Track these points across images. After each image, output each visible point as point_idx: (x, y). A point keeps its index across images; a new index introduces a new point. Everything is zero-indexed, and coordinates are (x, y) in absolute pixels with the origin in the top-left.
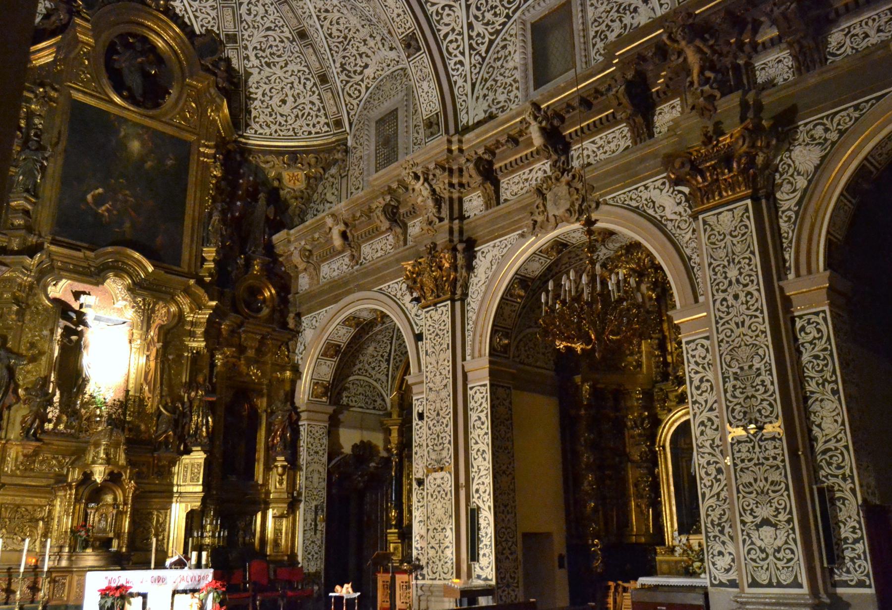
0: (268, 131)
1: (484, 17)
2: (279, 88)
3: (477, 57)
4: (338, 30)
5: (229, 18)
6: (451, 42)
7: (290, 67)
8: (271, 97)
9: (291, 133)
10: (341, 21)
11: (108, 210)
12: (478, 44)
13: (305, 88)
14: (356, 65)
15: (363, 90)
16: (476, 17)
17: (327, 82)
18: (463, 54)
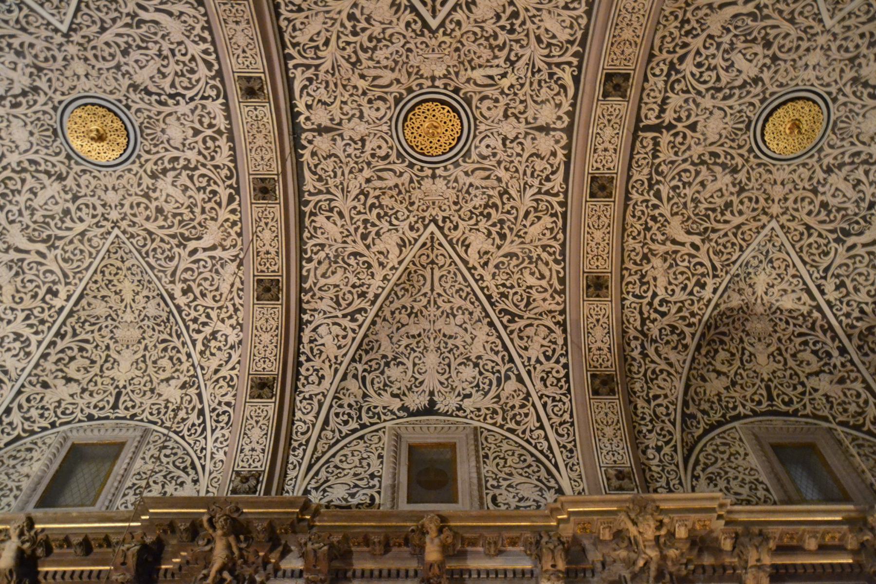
1: (28, 410)
16: (20, 407)
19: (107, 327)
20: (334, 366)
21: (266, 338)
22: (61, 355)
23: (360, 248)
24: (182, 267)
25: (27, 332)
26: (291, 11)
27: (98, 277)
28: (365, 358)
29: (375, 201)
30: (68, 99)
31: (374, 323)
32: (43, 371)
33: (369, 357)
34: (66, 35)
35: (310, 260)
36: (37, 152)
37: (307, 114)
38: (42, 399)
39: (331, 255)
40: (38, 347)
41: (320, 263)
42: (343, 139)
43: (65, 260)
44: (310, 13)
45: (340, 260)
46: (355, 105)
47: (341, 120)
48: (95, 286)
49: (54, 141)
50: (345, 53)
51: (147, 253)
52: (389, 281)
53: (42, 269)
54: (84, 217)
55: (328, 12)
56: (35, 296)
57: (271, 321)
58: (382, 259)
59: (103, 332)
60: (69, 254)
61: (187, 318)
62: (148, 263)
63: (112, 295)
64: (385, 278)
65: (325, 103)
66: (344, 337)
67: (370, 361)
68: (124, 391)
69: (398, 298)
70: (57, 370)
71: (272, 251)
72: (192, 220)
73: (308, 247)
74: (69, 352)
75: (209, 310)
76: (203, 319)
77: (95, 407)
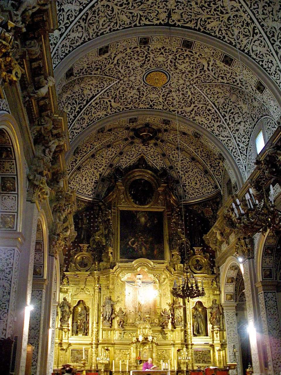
0: (194, 196)
3: (244, 156)
5: (168, 161)
6: (234, 152)
7: (194, 171)
9: (202, 195)
10: (204, 150)
11: (136, 246)
13: (201, 176)
14: (215, 163)
16: (239, 141)
18: (239, 156)
20: (270, 54)
22: (231, 120)
23: (227, 16)
25: (218, 124)
26: (116, 26)
27: (209, 96)
28: (275, 39)
29: (207, 4)
30: (143, 82)
31: (262, 26)
33: (276, 36)
34: (121, 80)
35: (224, 37)
36: (160, 94)
37: (161, 21)
39: (226, 28)
41: (227, 34)
42: (175, 9)
43: (200, 102)
44: (118, 20)
45: (229, 26)
46: (160, 3)
47: (166, 9)
48: (212, 98)
50: (137, 7)
52: (246, 11)
53: (200, 108)
54: (186, 91)
55: (118, 13)
56: (209, 115)
58: (235, 9)
59: (230, 104)
62: (208, 82)
64: (245, 12)
65: (157, 14)
66: (261, 42)
67: (278, 36)
69: (257, 8)
71: (213, 51)
72: (196, 65)
73: (218, 35)
74: (231, 117)
76: (234, 80)
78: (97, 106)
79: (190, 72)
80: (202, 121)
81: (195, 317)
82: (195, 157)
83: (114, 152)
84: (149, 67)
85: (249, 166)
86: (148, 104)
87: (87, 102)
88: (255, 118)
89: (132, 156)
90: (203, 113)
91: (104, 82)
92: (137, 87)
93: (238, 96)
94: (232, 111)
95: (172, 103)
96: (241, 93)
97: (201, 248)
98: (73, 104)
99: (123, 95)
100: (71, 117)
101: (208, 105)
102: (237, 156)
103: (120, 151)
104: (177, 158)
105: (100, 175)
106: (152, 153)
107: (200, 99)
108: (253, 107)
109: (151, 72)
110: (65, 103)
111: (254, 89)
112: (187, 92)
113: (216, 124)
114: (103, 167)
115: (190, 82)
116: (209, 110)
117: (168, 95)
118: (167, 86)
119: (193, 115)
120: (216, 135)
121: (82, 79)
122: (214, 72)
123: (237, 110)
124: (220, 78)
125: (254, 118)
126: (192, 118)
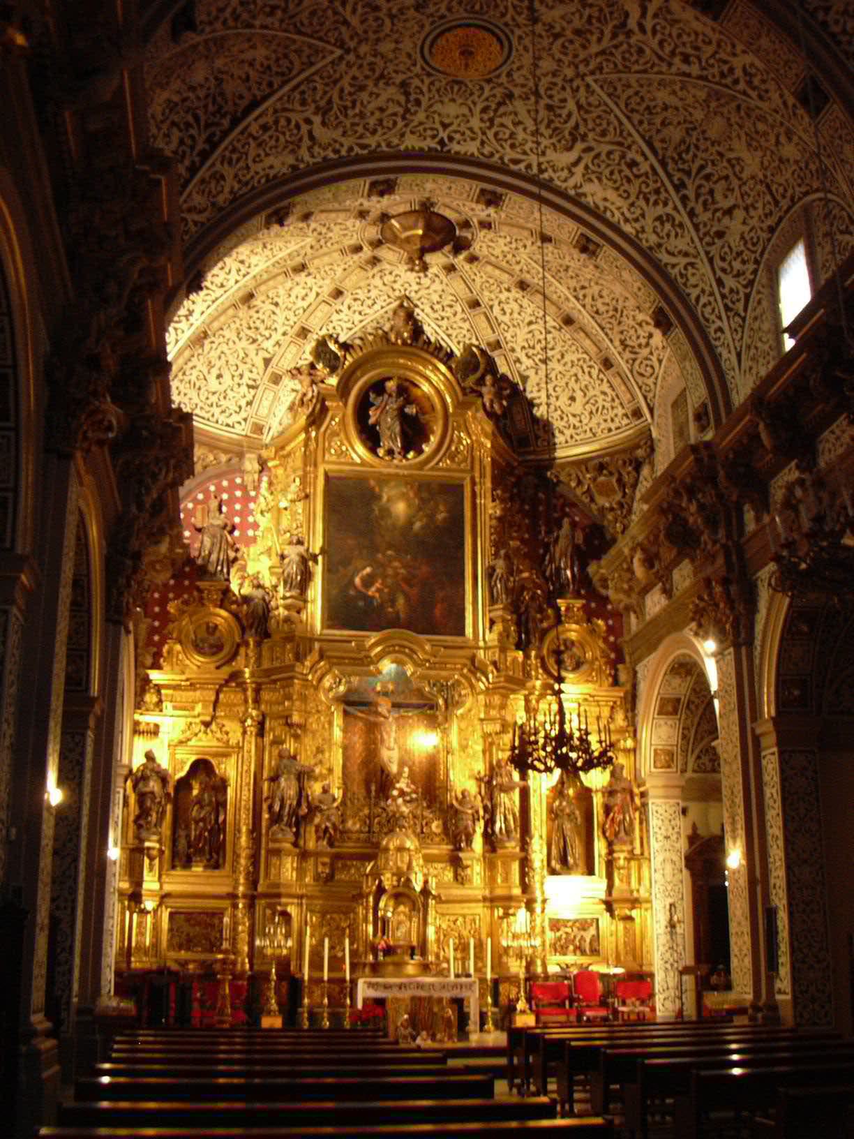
2: (563, 383)
3: (737, 319)
4: (604, 304)
5: (485, 324)
6: (705, 306)
7: (568, 358)
8: (557, 398)
9: (589, 434)
10: (605, 293)
11: (378, 590)
12: (733, 303)
14: (638, 337)
15: (656, 364)
17: (612, 366)
18: (720, 318)
19: (698, 140)
21: (764, 42)
22: (701, 199)
24: (656, 47)
25: (660, 210)
27: (636, 117)
30: (420, 62)
32: (705, 225)
34: (348, 51)
36: (475, 104)
38: (730, 247)
40: (678, 212)
48: (645, 125)
49: (466, 86)
51: (626, 67)
53: (603, 157)
54: (561, 97)
56: (629, 181)
57: (752, 22)
59: (702, 147)
60: (598, 130)
61: (717, 79)
63: (665, 114)
68: (768, 181)
70: (714, 214)
72: (601, 10)
74: (703, 190)
75: (717, 56)
76: (725, 68)
77: (766, 216)
78: (266, 137)
79: (578, 32)
80: (605, 199)
81: (557, 816)
82: (575, 315)
83: (315, 289)
84: (443, 11)
85: (753, 351)
86: (434, 137)
87: (235, 122)
88: (784, 197)
89: (370, 302)
90: (612, 173)
91: (293, 56)
92: (399, 78)
93: (733, 120)
94: (708, 170)
95: (512, 135)
96: (742, 113)
97: (578, 603)
98: (188, 125)
99: (354, 103)
100: (182, 169)
101: (629, 147)
102: (713, 317)
103: (332, 287)
104: (515, 315)
105: (267, 362)
106: (435, 298)
107: (605, 125)
108: (781, 160)
109: (449, 29)
110: (162, 122)
111: (791, 101)
112: (564, 100)
113: (653, 212)
114: (277, 337)
115: (577, 67)
116: (633, 164)
117: (502, 110)
118: (498, 76)
119: (577, 178)
120: (651, 248)
121: (220, 43)
122: (659, 36)
123: (722, 168)
124: (677, 60)
125: (779, 198)
126: (575, 187)
